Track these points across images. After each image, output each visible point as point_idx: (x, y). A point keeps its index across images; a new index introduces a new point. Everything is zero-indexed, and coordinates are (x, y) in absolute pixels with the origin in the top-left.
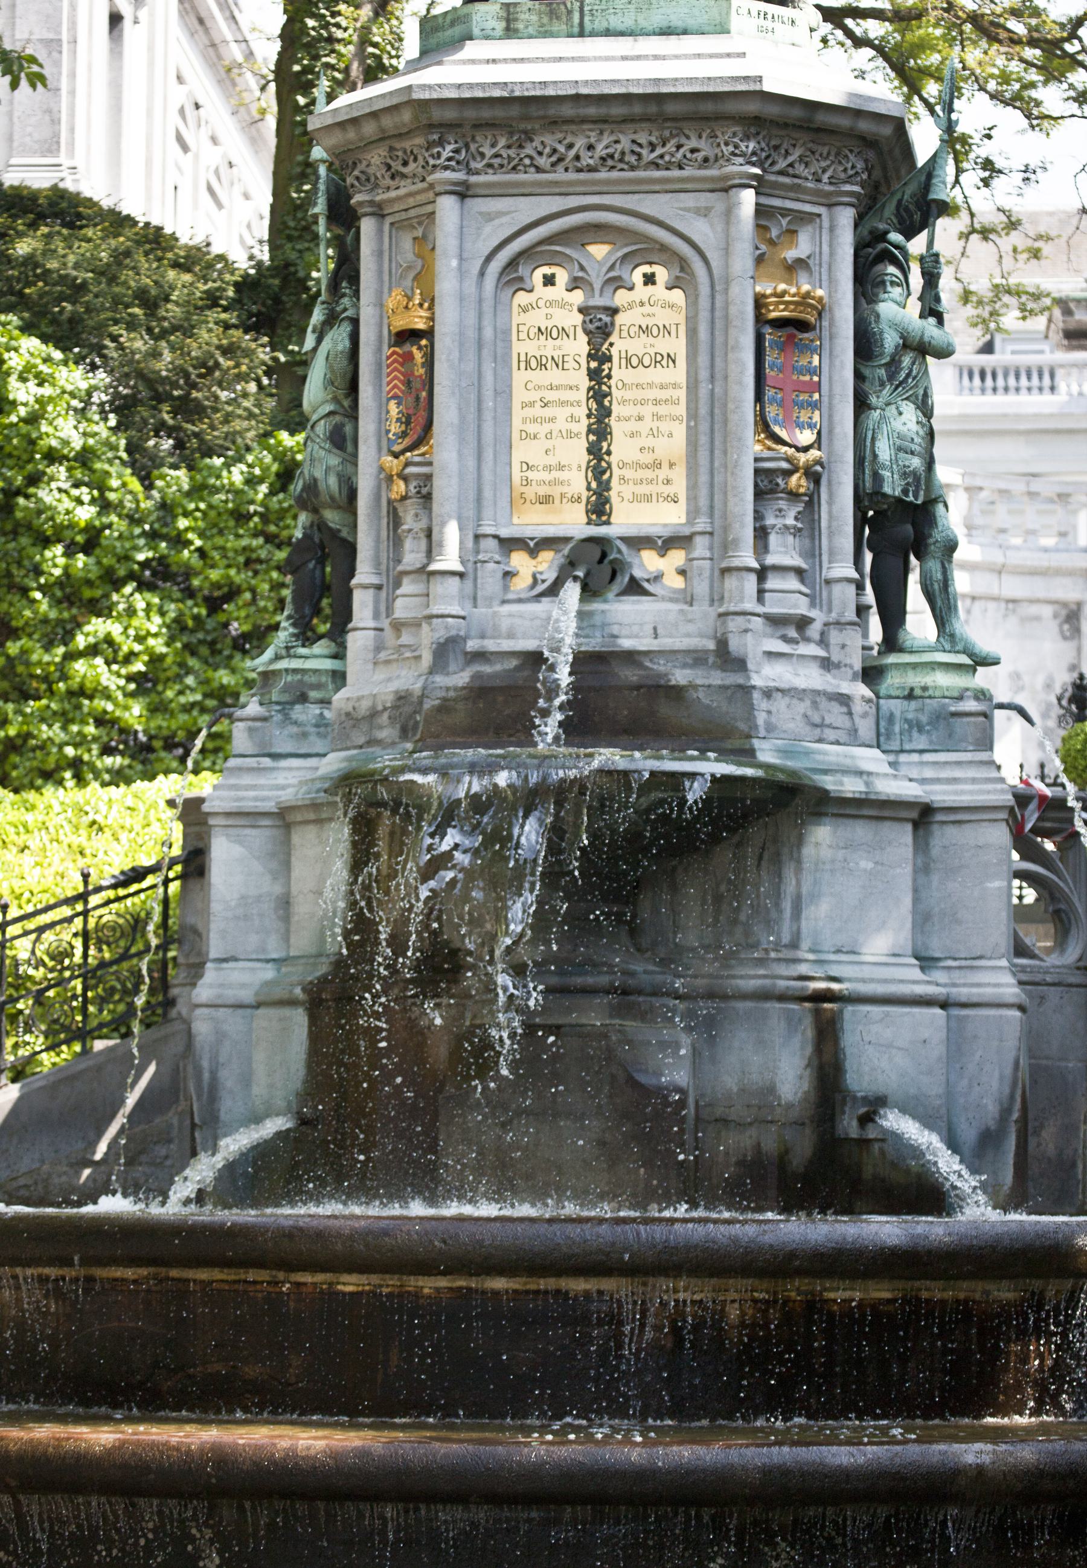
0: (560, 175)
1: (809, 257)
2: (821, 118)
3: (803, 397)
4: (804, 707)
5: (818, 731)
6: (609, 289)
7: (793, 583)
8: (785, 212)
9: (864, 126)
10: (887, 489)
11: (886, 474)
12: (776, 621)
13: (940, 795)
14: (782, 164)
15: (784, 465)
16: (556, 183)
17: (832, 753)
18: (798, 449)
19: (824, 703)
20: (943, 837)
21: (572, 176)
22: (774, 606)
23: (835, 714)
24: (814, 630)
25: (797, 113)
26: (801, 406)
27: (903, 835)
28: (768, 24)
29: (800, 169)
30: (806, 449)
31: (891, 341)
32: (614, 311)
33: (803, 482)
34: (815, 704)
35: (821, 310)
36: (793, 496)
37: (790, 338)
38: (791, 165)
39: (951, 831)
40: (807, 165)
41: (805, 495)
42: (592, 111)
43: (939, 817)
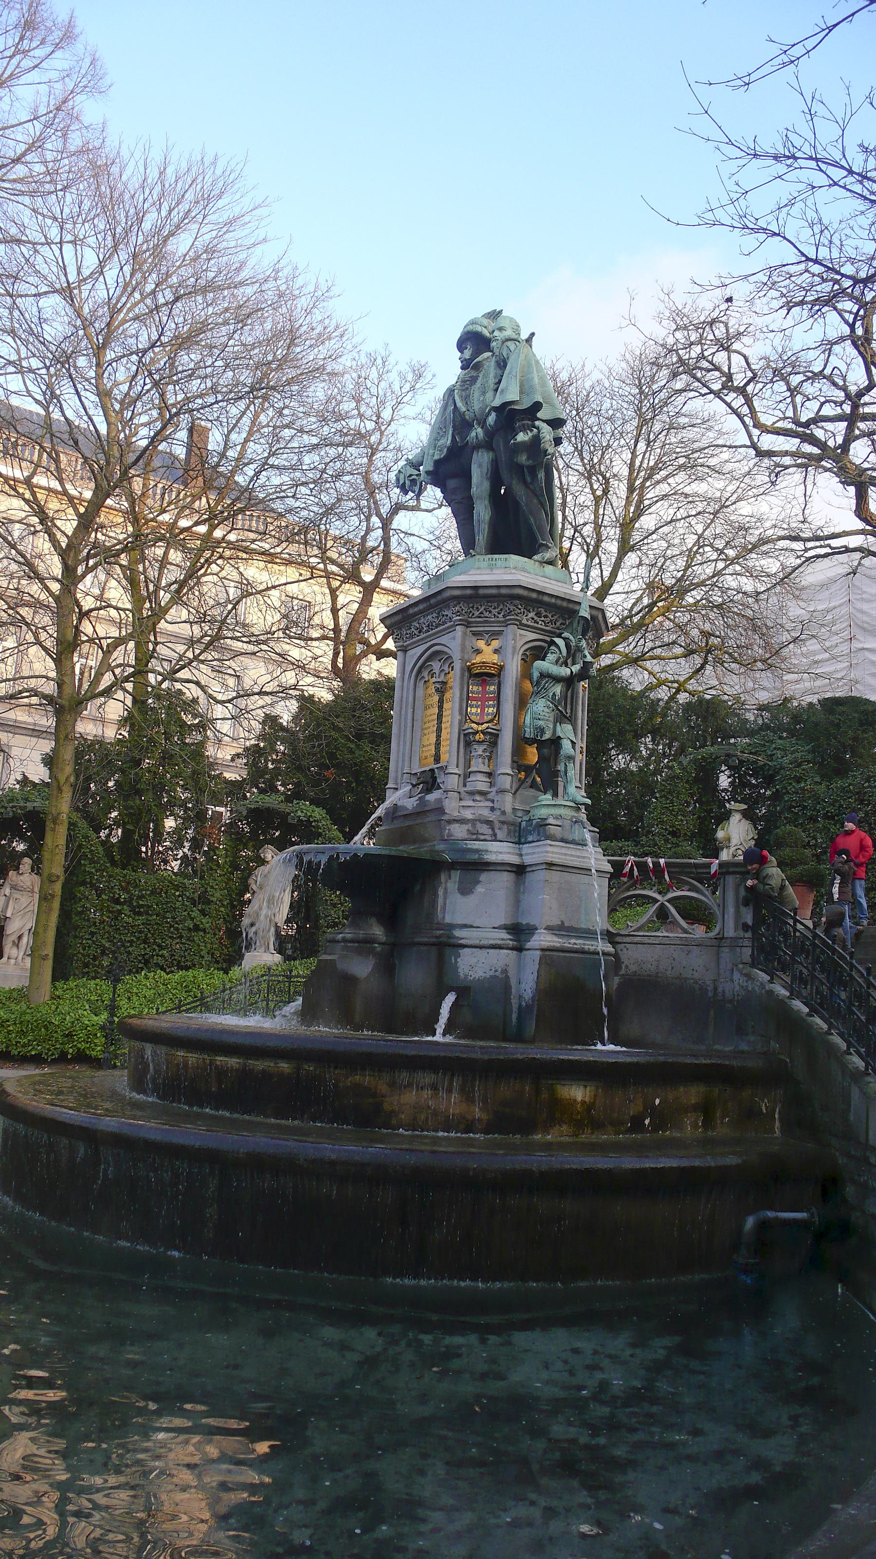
0: (423, 636)
1: (501, 648)
2: (481, 592)
3: (491, 703)
4: (469, 826)
5: (475, 837)
6: (443, 675)
7: (480, 777)
8: (487, 632)
9: (504, 591)
10: (526, 736)
11: (528, 730)
12: (471, 793)
13: (528, 860)
14: (477, 613)
15: (470, 731)
16: (422, 639)
17: (476, 845)
18: (477, 724)
19: (479, 825)
20: (530, 877)
21: (425, 635)
22: (468, 788)
23: (484, 829)
24: (489, 796)
25: (468, 592)
26: (489, 707)
27: (505, 879)
28: (494, 562)
29: (487, 614)
30: (482, 724)
31: (536, 675)
32: (444, 683)
33: (482, 736)
34: (474, 825)
35: (501, 668)
36: (480, 742)
37: (484, 681)
38: (481, 613)
39: (531, 874)
40: (490, 612)
41: (483, 741)
42: (416, 609)
43: (528, 869)
